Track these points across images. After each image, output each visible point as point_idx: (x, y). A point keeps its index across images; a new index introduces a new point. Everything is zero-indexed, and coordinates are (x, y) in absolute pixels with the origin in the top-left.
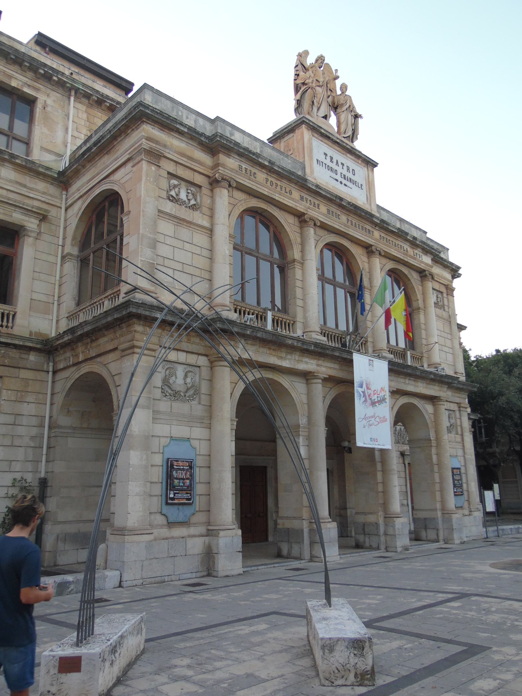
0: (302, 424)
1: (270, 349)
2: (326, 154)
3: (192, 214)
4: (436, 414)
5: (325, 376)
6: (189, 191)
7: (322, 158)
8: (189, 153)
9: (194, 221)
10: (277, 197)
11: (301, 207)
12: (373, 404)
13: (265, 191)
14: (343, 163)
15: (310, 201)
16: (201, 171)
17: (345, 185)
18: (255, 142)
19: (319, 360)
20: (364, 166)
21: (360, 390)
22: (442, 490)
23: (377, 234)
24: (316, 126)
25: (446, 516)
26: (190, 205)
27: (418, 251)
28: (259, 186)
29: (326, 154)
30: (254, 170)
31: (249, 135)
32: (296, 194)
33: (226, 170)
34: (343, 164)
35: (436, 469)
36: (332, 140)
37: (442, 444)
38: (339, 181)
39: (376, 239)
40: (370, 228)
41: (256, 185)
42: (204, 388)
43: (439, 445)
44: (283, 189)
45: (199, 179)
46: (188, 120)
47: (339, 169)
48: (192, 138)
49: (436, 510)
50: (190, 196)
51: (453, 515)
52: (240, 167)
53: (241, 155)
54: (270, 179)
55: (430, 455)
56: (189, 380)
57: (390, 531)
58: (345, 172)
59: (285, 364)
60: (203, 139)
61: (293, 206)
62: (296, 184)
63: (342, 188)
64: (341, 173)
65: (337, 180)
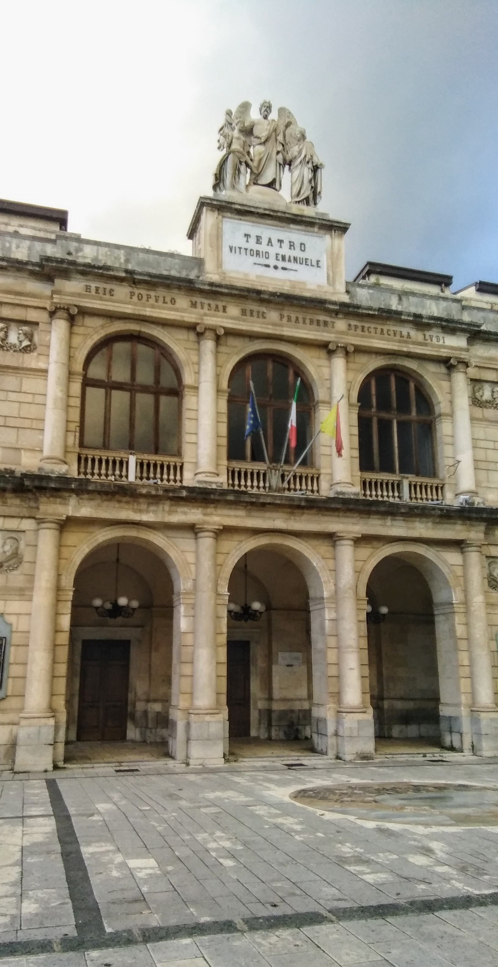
0: (185, 589)
1: (119, 502)
2: (247, 236)
3: (21, 359)
4: (464, 566)
5: (217, 527)
6: (21, 332)
7: (240, 242)
8: (18, 288)
9: (25, 366)
10: (148, 312)
11: (190, 317)
13: (128, 309)
14: (280, 239)
15: (209, 305)
16: (35, 304)
17: (284, 269)
18: (116, 251)
19: (207, 507)
20: (325, 234)
22: (471, 677)
23: (341, 324)
24: (224, 204)
25: (475, 714)
26: (21, 348)
27: (434, 333)
28: (116, 304)
29: (247, 236)
30: (108, 287)
31: (107, 245)
32: (183, 302)
33: (63, 297)
34: (281, 241)
35: (463, 645)
36: (258, 213)
37: (472, 609)
38: (272, 265)
39: (342, 333)
40: (328, 319)
41: (113, 304)
42: (27, 557)
43: (467, 613)
44: (161, 299)
45: (32, 315)
46: (19, 250)
47: (273, 250)
48: (19, 270)
49: (458, 705)
50: (22, 337)
51: (483, 715)
52: (88, 288)
53: (83, 273)
54: (137, 291)
55: (453, 625)
56: (7, 548)
57: (341, 733)
58: (285, 250)
59: (145, 518)
60: (30, 267)
61: (178, 318)
62: (179, 288)
63: (280, 274)
64: (277, 254)
65: (267, 266)
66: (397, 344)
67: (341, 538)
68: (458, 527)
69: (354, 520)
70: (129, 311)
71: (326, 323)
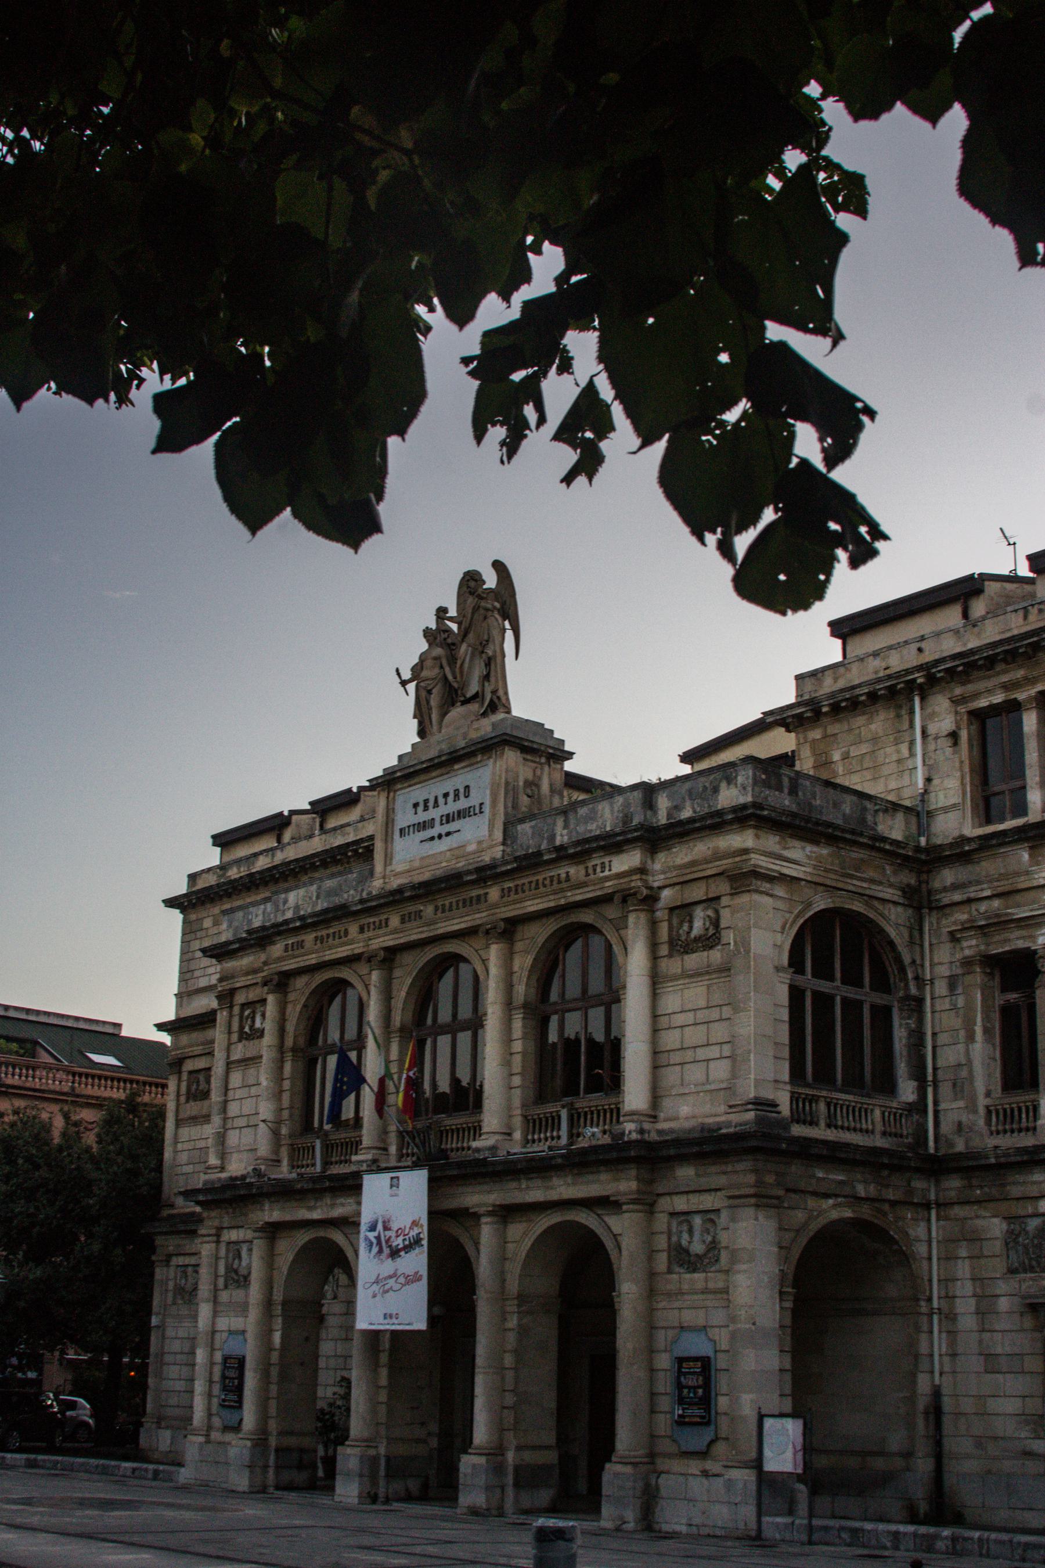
12: (395, 1253)
21: (372, 1235)
28: (306, 958)
40: (481, 892)
66: (552, 897)
67: (476, 1216)
68: (603, 1177)
69: (486, 1187)
70: (314, 962)
71: (479, 897)
